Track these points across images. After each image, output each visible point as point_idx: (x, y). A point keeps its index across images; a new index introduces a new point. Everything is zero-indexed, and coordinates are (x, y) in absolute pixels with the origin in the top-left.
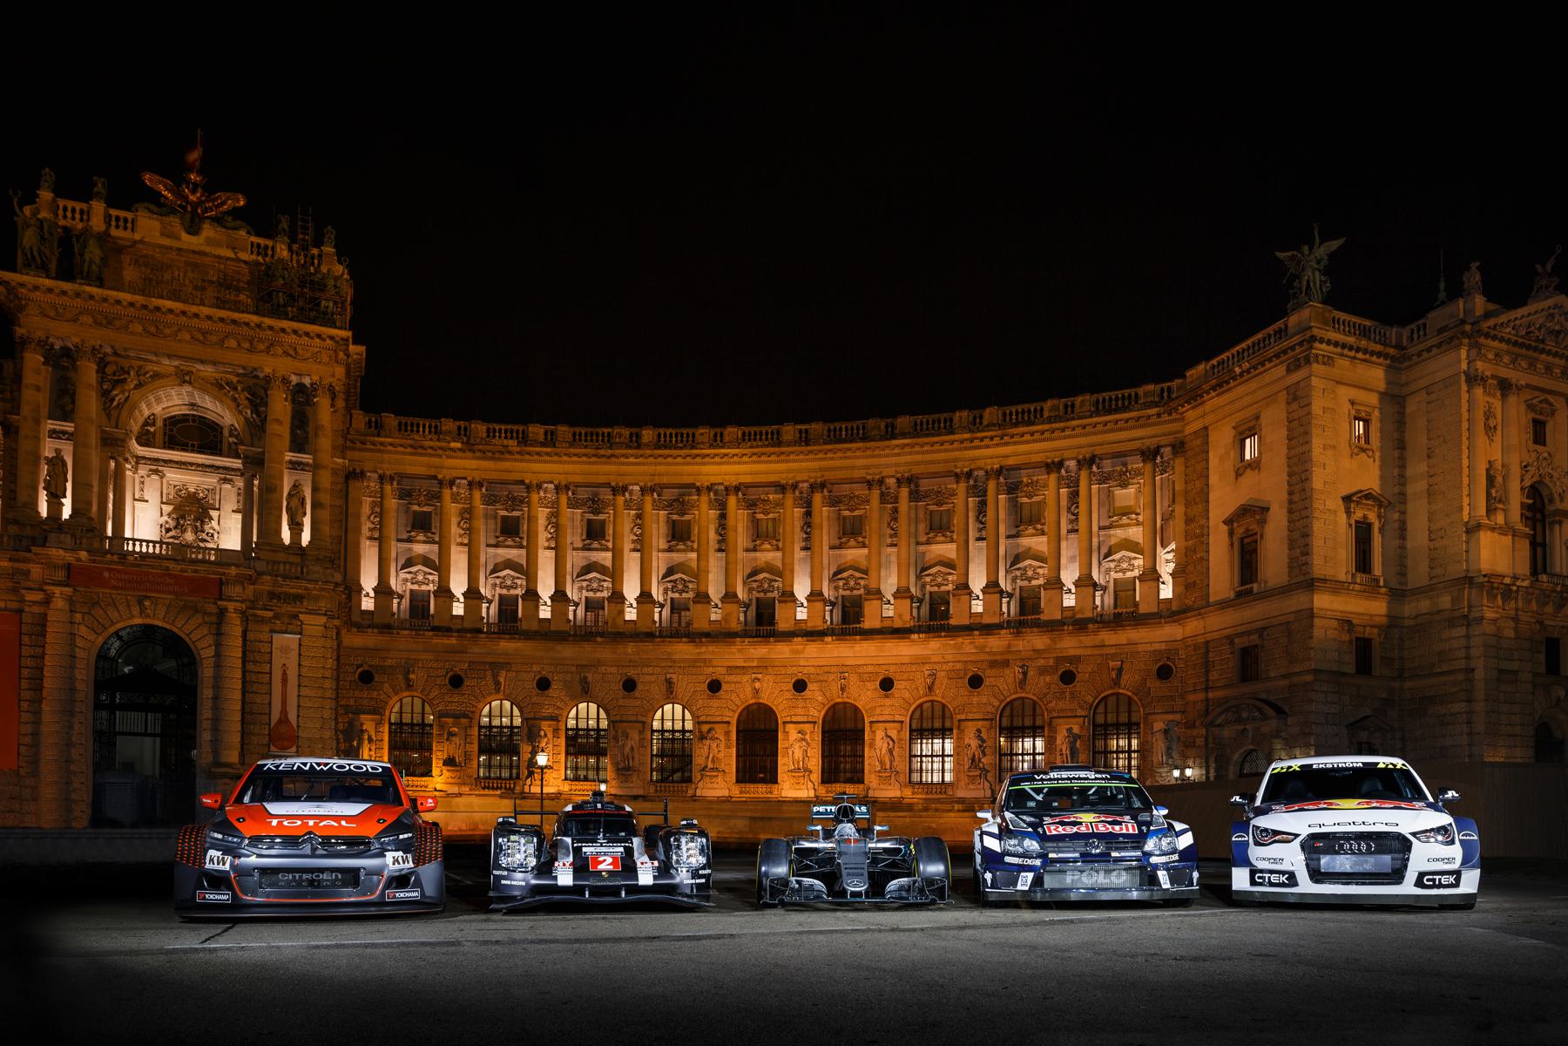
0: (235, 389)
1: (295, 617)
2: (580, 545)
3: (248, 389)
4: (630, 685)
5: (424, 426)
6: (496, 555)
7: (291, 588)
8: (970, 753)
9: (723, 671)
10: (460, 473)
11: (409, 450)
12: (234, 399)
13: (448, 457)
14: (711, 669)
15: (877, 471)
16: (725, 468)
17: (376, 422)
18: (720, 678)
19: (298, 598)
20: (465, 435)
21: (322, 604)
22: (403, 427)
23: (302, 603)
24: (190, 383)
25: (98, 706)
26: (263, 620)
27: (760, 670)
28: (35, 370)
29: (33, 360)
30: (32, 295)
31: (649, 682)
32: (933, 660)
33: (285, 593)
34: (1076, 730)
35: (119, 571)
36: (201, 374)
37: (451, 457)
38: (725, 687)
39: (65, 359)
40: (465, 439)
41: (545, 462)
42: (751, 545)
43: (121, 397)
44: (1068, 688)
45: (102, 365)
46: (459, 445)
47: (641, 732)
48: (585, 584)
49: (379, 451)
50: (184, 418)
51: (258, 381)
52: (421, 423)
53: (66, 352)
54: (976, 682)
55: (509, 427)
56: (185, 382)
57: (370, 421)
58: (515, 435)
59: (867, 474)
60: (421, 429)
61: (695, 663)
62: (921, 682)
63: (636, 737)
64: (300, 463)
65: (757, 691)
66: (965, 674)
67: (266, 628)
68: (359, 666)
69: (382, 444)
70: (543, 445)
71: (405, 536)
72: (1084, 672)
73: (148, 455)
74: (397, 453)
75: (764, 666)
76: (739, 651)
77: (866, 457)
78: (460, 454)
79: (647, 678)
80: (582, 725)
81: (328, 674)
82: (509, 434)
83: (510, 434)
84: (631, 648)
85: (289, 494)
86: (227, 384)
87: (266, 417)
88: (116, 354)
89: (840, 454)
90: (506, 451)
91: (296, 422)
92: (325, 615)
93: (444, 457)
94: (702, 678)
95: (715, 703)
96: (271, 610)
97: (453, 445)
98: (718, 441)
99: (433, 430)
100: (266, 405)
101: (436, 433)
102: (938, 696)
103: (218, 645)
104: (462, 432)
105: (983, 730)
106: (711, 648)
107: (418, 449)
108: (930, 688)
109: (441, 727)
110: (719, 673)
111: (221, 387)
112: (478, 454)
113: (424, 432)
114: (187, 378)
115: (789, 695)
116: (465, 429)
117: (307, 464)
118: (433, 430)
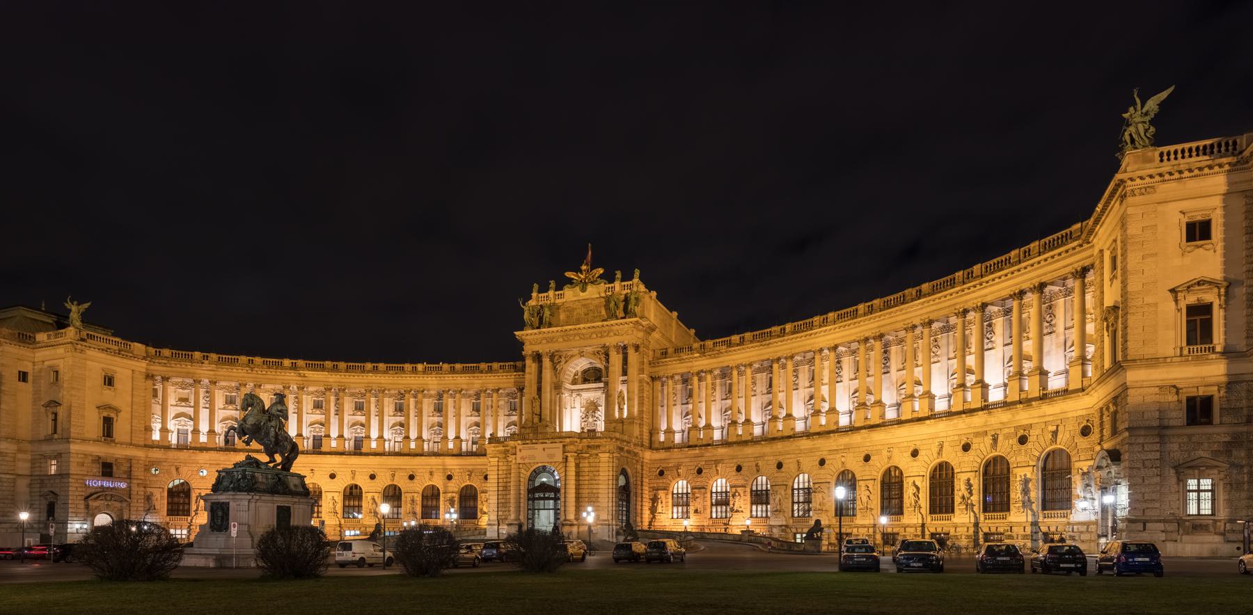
1: (597, 455)
2: (766, 392)
4: (780, 466)
6: (726, 404)
8: (960, 494)
9: (826, 453)
12: (600, 358)
13: (695, 361)
14: (820, 453)
15: (910, 322)
16: (828, 337)
18: (824, 457)
19: (598, 446)
21: (607, 447)
24: (583, 356)
25: (529, 499)
26: (585, 458)
27: (847, 451)
28: (531, 366)
29: (529, 362)
30: (527, 337)
31: (789, 465)
32: (941, 436)
33: (594, 446)
34: (1029, 476)
37: (697, 361)
38: (827, 462)
42: (853, 376)
44: (1023, 447)
45: (552, 357)
47: (785, 490)
48: (767, 412)
49: (666, 365)
50: (588, 370)
54: (966, 448)
56: (581, 356)
59: (904, 324)
61: (811, 450)
62: (935, 449)
63: (783, 493)
65: (843, 463)
66: (960, 443)
68: (658, 468)
69: (666, 362)
71: (685, 402)
72: (1033, 435)
73: (575, 388)
75: (847, 448)
76: (834, 441)
77: (903, 314)
79: (788, 461)
80: (759, 488)
81: (611, 478)
84: (779, 446)
85: (619, 397)
89: (887, 316)
94: (815, 458)
95: (822, 471)
98: (824, 323)
102: (944, 458)
103: (566, 471)
105: (971, 478)
106: (819, 441)
107: (682, 361)
108: (940, 453)
109: (694, 494)
110: (824, 455)
115: (861, 464)
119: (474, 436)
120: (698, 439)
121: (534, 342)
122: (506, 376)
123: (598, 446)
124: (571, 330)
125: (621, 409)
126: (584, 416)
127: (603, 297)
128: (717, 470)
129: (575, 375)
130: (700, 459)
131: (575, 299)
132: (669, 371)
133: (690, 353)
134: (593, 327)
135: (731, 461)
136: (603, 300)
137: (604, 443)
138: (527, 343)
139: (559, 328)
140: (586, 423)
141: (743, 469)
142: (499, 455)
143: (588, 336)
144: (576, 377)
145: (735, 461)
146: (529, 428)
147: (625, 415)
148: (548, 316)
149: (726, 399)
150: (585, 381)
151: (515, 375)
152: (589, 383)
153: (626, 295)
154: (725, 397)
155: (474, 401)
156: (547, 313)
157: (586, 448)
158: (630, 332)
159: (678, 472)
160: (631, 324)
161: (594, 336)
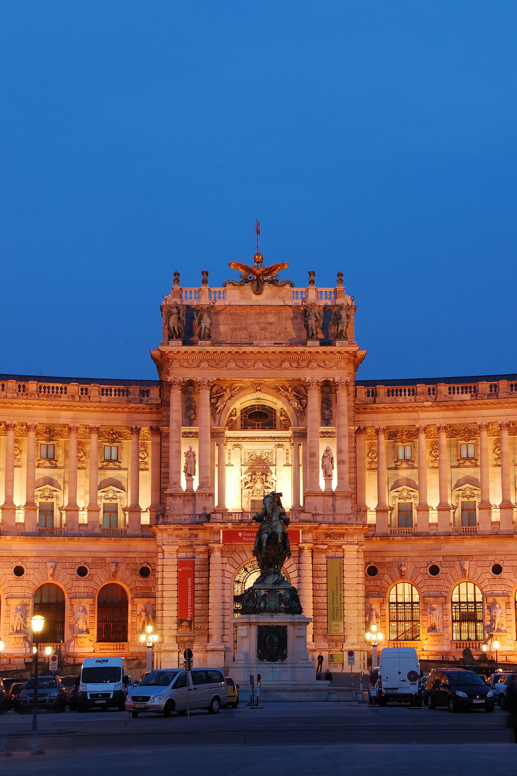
0: (287, 390)
1: (340, 546)
3: (295, 389)
5: (405, 390)
7: (336, 529)
10: (431, 422)
11: (396, 409)
12: (286, 397)
17: (373, 391)
20: (434, 394)
22: (391, 393)
23: (343, 538)
24: (260, 391)
26: (322, 551)
35: (247, 532)
36: (266, 383)
37: (425, 411)
39: (190, 388)
40: (434, 397)
41: (491, 408)
43: (222, 406)
46: (430, 403)
49: (375, 413)
51: (300, 383)
52: (403, 389)
53: (191, 383)
55: (464, 385)
56: (257, 390)
57: (368, 392)
58: (468, 390)
60: (403, 393)
64: (327, 433)
67: (323, 556)
69: (378, 408)
70: (490, 396)
74: (387, 412)
78: (431, 409)
82: (464, 390)
83: (465, 390)
85: (323, 456)
86: (282, 387)
87: (306, 405)
88: (218, 380)
90: (461, 405)
91: (325, 406)
92: (357, 544)
93: (420, 411)
96: (326, 544)
97: (426, 404)
99: (411, 393)
100: (306, 397)
101: (413, 395)
104: (432, 392)
107: (401, 409)
111: (278, 390)
112: (444, 407)
113: (405, 395)
114: (259, 388)
116: (434, 389)
117: (332, 433)
118: (411, 393)
119: (44, 500)
120: (430, 525)
121: (186, 365)
122: (115, 408)
123: (342, 535)
124: (251, 352)
125: (328, 476)
126: (249, 479)
127: (290, 306)
128: (464, 571)
129: (231, 415)
130: (434, 553)
131: (243, 303)
132: (380, 422)
133: (413, 398)
134: (288, 352)
135: (484, 558)
136: (290, 310)
137: (352, 531)
138: (176, 364)
139: (234, 349)
140: (251, 491)
141: (504, 570)
142: (180, 543)
143: (276, 364)
144: (234, 418)
145: (490, 558)
146: (180, 496)
147: (334, 485)
148: (208, 326)
149: (458, 467)
150: (245, 426)
151: (131, 408)
152: (253, 429)
153: (325, 307)
154: (456, 464)
155: (44, 442)
156: (206, 322)
157: (323, 537)
158: (343, 364)
159: (401, 572)
160: (346, 354)
161: (286, 364)
